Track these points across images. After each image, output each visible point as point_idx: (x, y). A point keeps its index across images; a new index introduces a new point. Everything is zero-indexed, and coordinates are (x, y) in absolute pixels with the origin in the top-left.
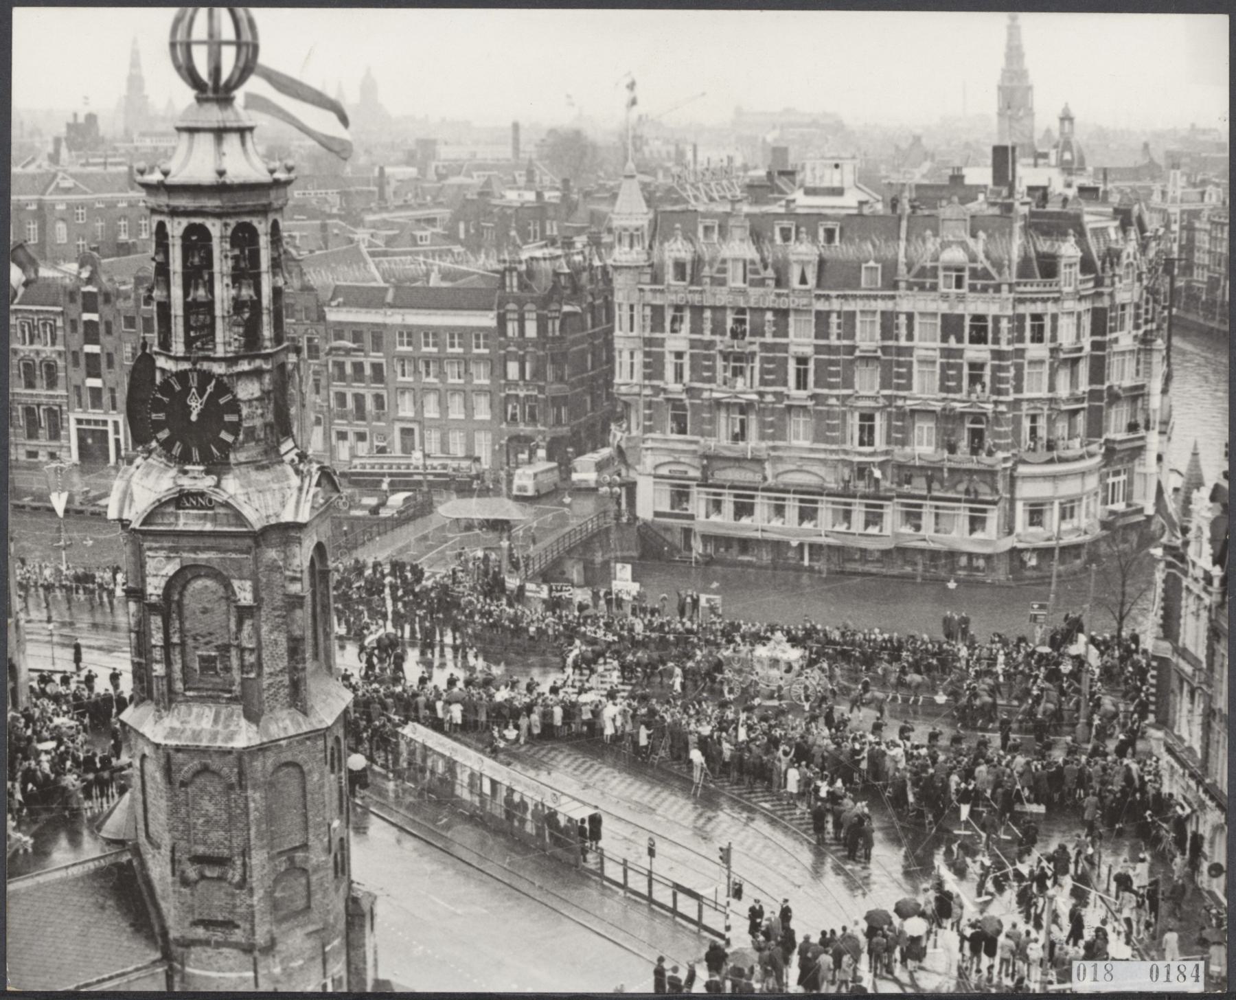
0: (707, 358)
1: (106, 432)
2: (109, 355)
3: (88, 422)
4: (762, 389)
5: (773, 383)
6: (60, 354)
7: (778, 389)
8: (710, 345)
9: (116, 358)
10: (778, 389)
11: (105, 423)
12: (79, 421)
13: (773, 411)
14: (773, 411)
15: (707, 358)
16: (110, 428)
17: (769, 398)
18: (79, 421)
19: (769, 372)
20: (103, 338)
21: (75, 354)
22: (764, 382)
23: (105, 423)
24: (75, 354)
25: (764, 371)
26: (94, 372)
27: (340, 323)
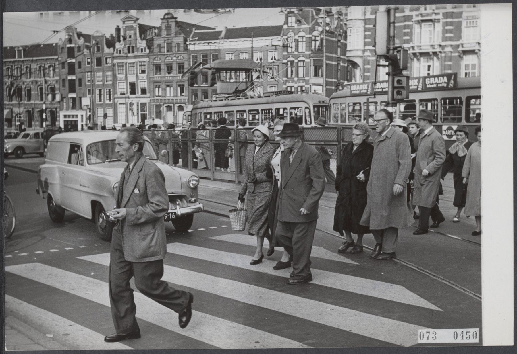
0: (408, 27)
1: (76, 122)
2: (80, 80)
3: (69, 116)
4: (443, 44)
5: (451, 39)
6: (57, 81)
7: (454, 43)
8: (409, 18)
9: (83, 81)
10: (454, 43)
11: (77, 116)
12: (65, 116)
13: (450, 59)
14: (450, 59)
15: (408, 27)
16: (79, 119)
17: (448, 49)
18: (65, 116)
19: (447, 31)
20: (77, 70)
21: (64, 80)
22: (445, 39)
23: (77, 116)
24: (64, 80)
25: (445, 31)
26: (72, 89)
27: (195, 51)
